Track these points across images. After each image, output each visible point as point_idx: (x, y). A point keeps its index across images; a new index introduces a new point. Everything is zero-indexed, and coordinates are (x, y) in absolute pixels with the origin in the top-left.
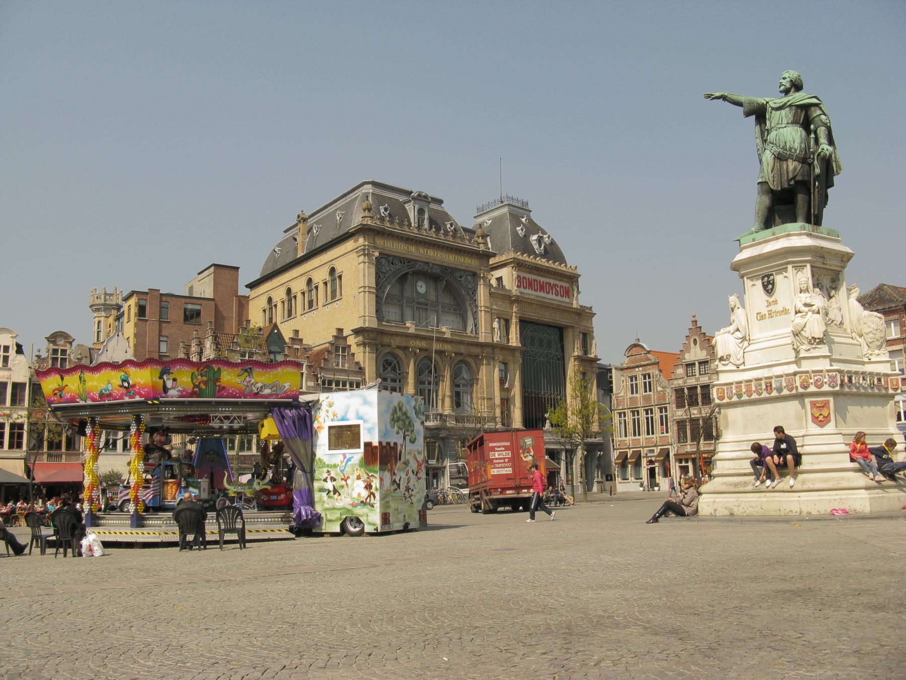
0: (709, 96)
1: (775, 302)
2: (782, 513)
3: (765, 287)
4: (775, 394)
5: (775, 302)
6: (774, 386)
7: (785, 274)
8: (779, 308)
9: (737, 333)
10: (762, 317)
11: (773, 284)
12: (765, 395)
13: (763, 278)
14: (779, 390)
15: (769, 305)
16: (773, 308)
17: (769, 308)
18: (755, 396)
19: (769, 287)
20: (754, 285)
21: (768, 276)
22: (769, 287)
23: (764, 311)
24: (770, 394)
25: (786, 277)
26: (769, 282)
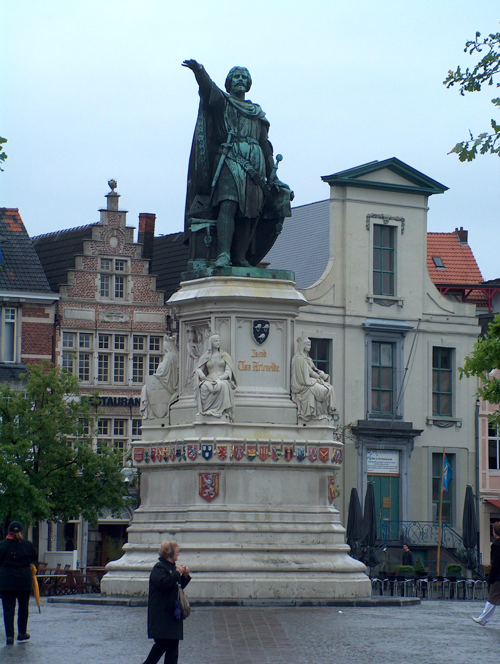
0: (192, 64)
1: (264, 354)
2: (337, 595)
3: (256, 333)
4: (294, 462)
5: (264, 354)
6: (295, 454)
7: (280, 326)
8: (266, 362)
9: (233, 383)
10: (247, 368)
11: (267, 334)
12: (282, 462)
13: (256, 323)
14: (301, 458)
15: (256, 355)
16: (260, 360)
17: (256, 360)
18: (271, 462)
19: (260, 334)
20: (240, 327)
21: (263, 323)
22: (260, 334)
23: (249, 361)
24: (288, 461)
25: (280, 329)
26: (262, 331)
